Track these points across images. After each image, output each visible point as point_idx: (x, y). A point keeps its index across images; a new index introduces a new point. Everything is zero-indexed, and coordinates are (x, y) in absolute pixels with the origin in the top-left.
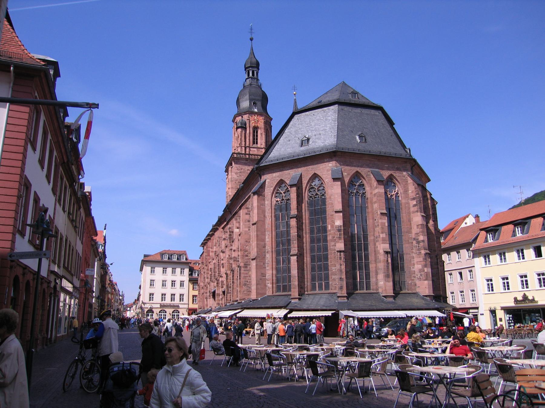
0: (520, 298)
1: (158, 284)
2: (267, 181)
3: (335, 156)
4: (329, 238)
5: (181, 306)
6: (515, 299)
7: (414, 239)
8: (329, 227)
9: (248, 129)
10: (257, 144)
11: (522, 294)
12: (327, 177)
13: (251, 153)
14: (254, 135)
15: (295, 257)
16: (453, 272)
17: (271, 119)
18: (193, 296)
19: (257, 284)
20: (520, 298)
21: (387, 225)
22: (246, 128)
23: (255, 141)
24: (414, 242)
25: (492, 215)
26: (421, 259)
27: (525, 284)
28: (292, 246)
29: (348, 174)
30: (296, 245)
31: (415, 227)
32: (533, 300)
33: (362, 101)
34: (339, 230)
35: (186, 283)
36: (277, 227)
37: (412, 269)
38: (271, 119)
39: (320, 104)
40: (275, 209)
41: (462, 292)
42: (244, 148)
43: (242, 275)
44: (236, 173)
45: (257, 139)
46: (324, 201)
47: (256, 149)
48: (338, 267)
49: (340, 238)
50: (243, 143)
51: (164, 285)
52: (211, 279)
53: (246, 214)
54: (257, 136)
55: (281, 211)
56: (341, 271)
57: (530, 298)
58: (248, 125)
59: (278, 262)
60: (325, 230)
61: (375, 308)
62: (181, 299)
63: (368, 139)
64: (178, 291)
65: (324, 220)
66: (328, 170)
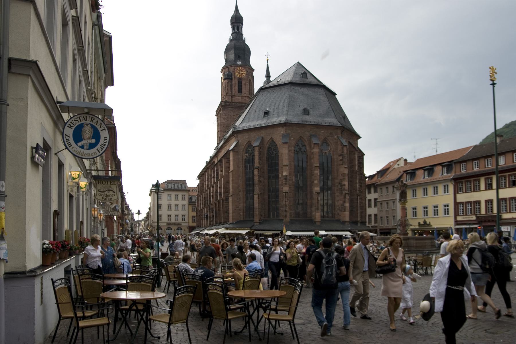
0: (422, 223)
1: (164, 207)
2: (240, 141)
3: (285, 126)
4: (280, 183)
5: (183, 224)
6: (419, 223)
7: (339, 183)
8: (280, 176)
9: (233, 80)
10: (241, 93)
11: (423, 220)
12: (279, 140)
13: (237, 101)
14: (239, 85)
15: (257, 196)
16: (389, 202)
17: (253, 70)
18: (193, 217)
19: (233, 213)
20: (422, 223)
21: (319, 174)
22: (232, 79)
23: (240, 91)
24: (339, 186)
25: (416, 159)
26: (343, 197)
27: (426, 213)
28: (255, 188)
29: (294, 139)
30: (258, 188)
31: (340, 175)
32: (429, 225)
33: (310, 80)
34: (286, 179)
35: (187, 207)
36: (246, 174)
37: (336, 204)
38: (253, 70)
39: (279, 83)
40: (245, 162)
41: (387, 217)
42: (230, 97)
43: (224, 206)
44: (224, 119)
45: (241, 89)
46: (277, 157)
47: (240, 98)
48: (284, 203)
49: (286, 184)
50: (230, 92)
51: (169, 208)
52: (205, 205)
53: (227, 162)
54: (241, 86)
55: (249, 163)
56: (286, 205)
57: (428, 223)
58: (233, 76)
59: (247, 199)
60: (277, 177)
61: (306, 229)
62: (183, 219)
63: (311, 112)
64: (180, 213)
65: (277, 171)
66: (280, 136)
